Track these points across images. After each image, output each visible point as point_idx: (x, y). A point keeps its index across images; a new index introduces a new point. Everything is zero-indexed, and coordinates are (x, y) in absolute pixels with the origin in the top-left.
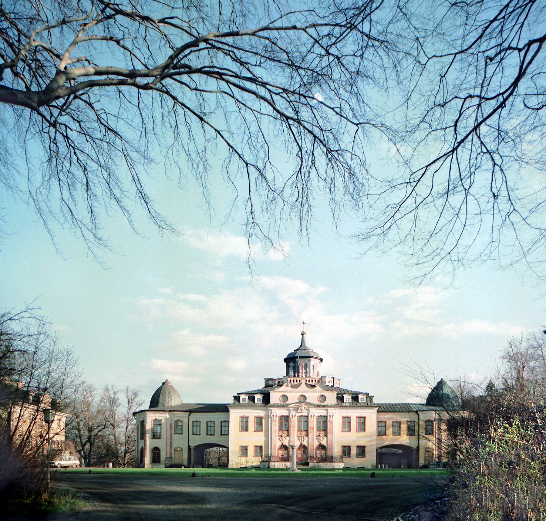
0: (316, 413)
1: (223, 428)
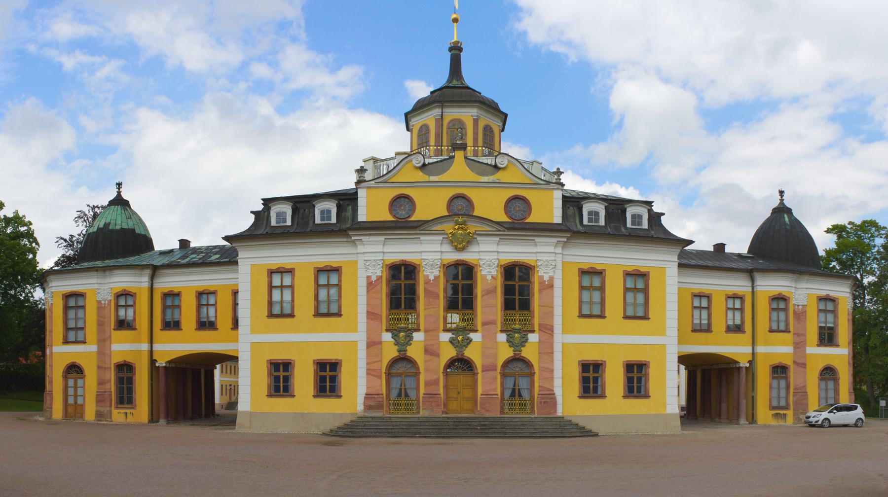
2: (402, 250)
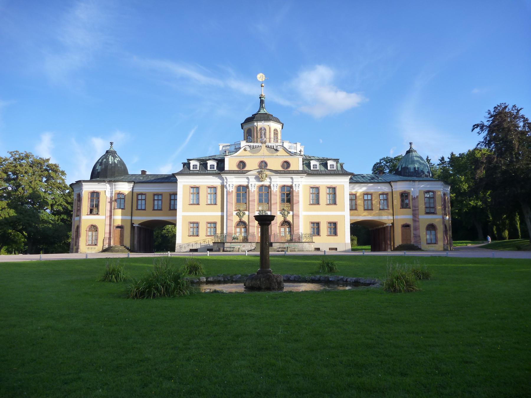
0: (277, 182)
1: (156, 202)
2: (242, 181)
